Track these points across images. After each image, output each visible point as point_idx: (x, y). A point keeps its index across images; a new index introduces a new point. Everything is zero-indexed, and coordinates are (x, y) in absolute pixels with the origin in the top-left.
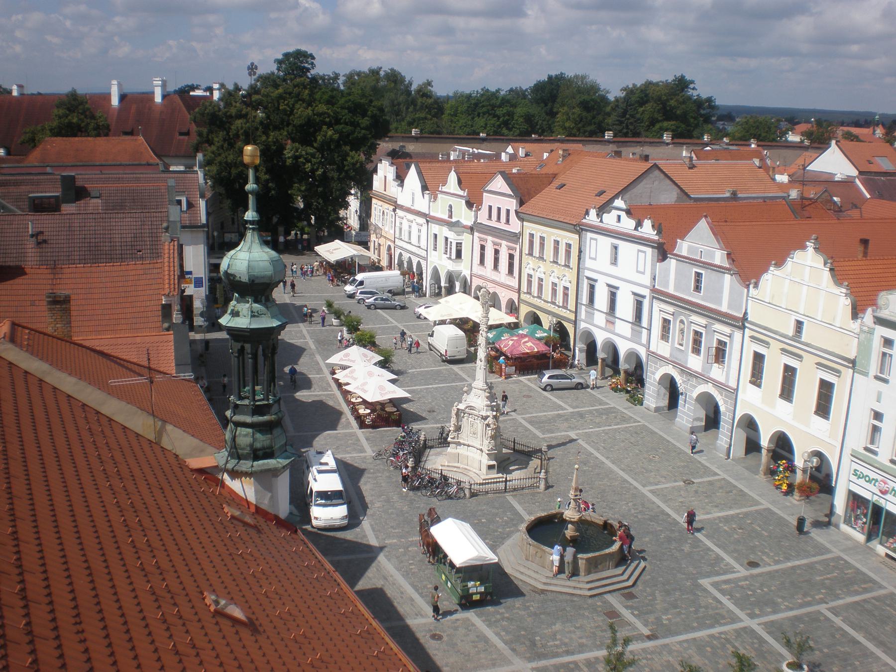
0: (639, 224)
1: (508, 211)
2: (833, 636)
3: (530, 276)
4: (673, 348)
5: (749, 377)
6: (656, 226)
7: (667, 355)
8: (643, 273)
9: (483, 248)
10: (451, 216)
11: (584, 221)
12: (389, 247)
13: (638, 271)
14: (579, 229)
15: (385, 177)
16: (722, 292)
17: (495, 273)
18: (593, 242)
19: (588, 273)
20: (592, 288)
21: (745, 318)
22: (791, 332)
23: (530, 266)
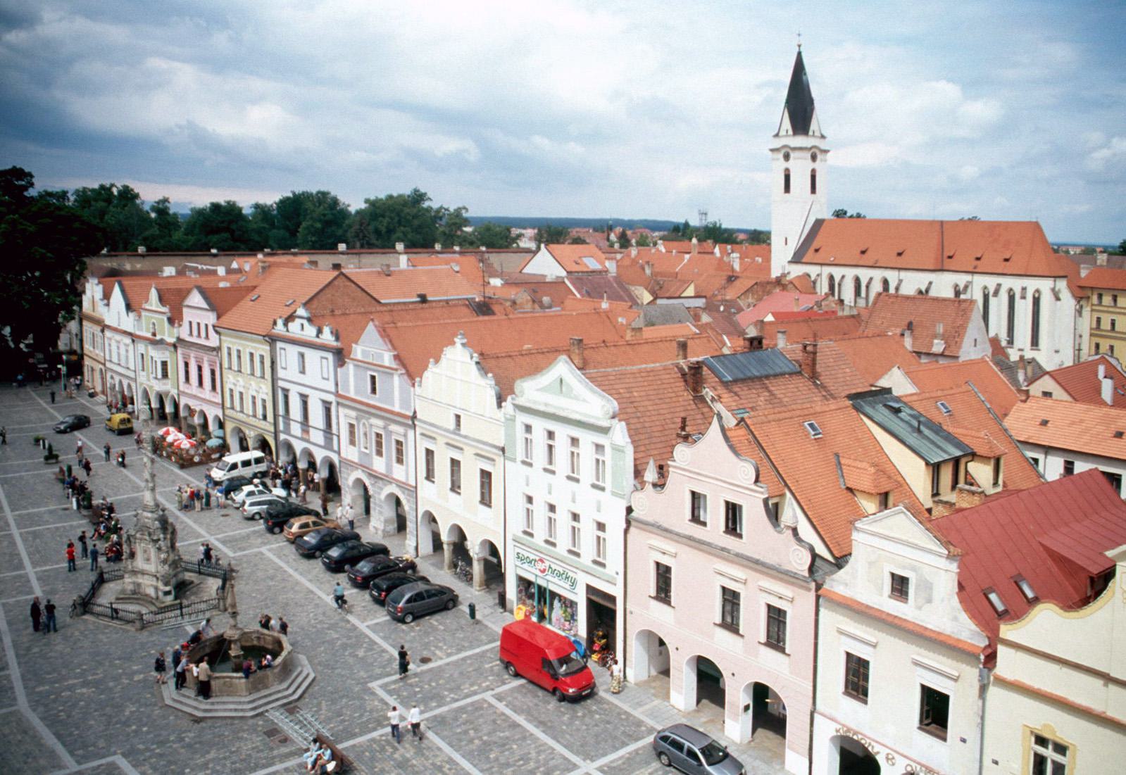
0: (320, 331)
1: (206, 325)
2: (494, 721)
3: (231, 390)
4: (361, 453)
5: (425, 475)
6: (334, 332)
7: (356, 460)
8: (328, 379)
9: (187, 365)
10: (154, 334)
11: (273, 331)
12: (101, 370)
13: (324, 378)
14: (272, 340)
15: (93, 297)
16: (392, 392)
17: (200, 390)
18: (283, 351)
19: (281, 384)
20: (286, 397)
21: (414, 417)
22: (451, 425)
23: (231, 381)
